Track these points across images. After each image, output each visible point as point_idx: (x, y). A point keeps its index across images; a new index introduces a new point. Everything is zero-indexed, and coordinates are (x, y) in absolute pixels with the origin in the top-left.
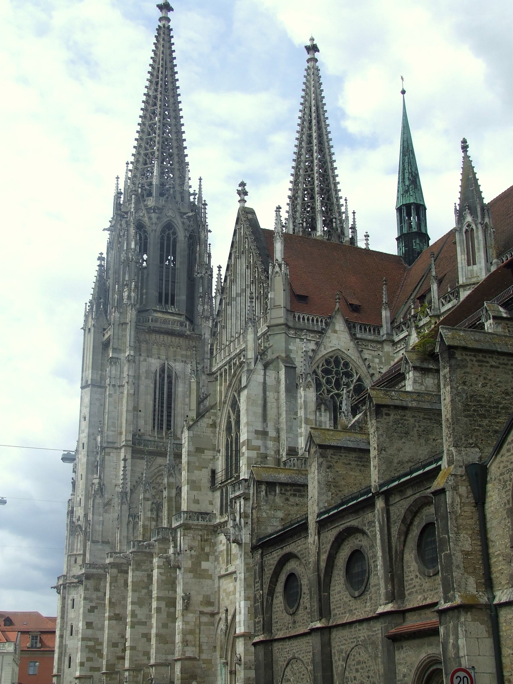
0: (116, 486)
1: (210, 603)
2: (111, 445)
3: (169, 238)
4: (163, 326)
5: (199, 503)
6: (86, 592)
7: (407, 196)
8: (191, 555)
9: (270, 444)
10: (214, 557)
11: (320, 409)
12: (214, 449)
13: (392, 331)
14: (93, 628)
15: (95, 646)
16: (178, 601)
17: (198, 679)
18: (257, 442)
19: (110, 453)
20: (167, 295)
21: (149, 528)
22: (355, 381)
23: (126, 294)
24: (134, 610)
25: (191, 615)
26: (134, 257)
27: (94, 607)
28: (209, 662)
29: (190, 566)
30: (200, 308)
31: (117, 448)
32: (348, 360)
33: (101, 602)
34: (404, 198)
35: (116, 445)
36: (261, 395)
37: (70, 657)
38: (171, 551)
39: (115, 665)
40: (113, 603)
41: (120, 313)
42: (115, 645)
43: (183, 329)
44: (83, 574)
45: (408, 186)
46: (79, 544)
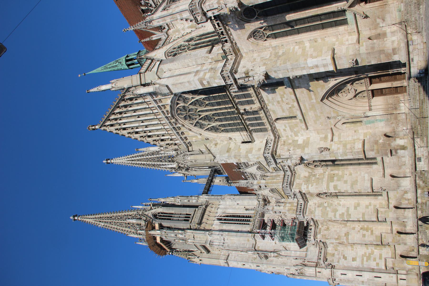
0: (276, 243)
1: (326, 138)
2: (254, 246)
3: (161, 216)
4: (198, 218)
5: (261, 148)
6: (334, 261)
7: (122, 63)
8: (293, 150)
9: (204, 68)
10: (295, 137)
11: (167, 10)
12: (230, 143)
13: (163, 32)
14: (356, 258)
15: (367, 257)
16: (325, 157)
17: (378, 139)
18: (201, 75)
19: (258, 247)
20: (186, 217)
21: (290, 207)
22: (184, 43)
23: (180, 236)
24: (339, 214)
25: (333, 147)
26: (164, 231)
27: (343, 257)
28: (365, 134)
29: (300, 150)
30: (194, 201)
31: (256, 243)
32: (172, 48)
33: (341, 253)
34: (123, 64)
35: (254, 243)
36: (174, 78)
37: (375, 277)
38: (289, 163)
39: (376, 236)
40: (338, 237)
41: (189, 239)
42: (364, 236)
43: (202, 209)
44: (324, 263)
45: (119, 63)
46: (310, 270)
